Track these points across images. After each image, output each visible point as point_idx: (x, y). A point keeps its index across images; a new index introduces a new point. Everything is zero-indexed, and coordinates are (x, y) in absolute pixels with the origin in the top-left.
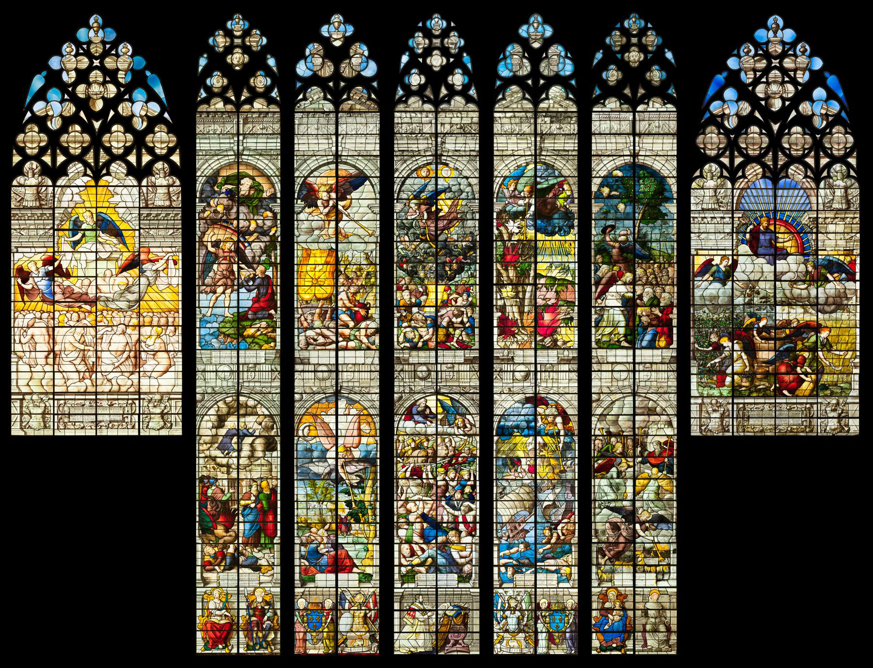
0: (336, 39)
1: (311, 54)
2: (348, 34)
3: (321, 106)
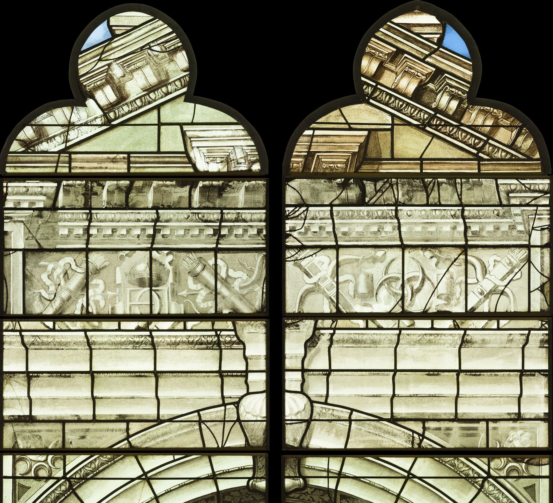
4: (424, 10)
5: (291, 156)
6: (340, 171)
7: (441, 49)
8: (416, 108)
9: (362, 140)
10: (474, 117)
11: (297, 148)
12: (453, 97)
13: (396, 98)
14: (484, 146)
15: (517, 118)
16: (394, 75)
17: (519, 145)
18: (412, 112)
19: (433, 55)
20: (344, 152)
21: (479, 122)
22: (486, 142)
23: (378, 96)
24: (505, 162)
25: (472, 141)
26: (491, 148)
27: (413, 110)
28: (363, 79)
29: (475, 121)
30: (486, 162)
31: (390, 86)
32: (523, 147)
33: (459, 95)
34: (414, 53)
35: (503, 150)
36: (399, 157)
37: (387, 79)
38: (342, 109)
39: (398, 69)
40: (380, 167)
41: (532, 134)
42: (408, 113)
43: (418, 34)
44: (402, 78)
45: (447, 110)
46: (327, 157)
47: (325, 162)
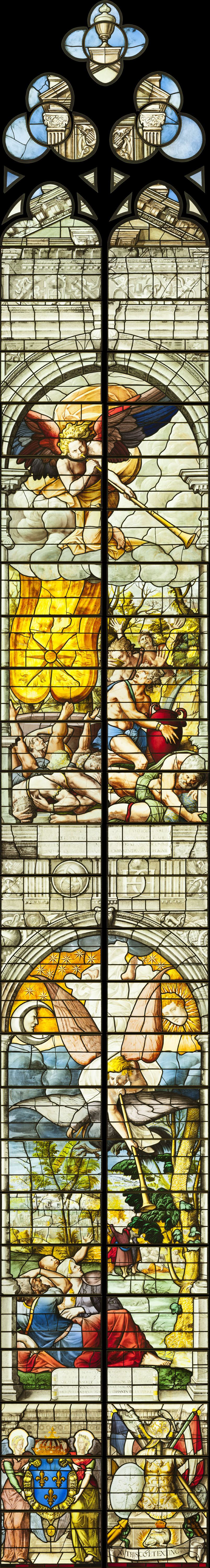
0: (102, 66)
1: (41, 103)
2: (132, 53)
3: (65, 233)
10: (180, 224)
12: (172, 217)
37: (147, 210)
41: (202, 230)
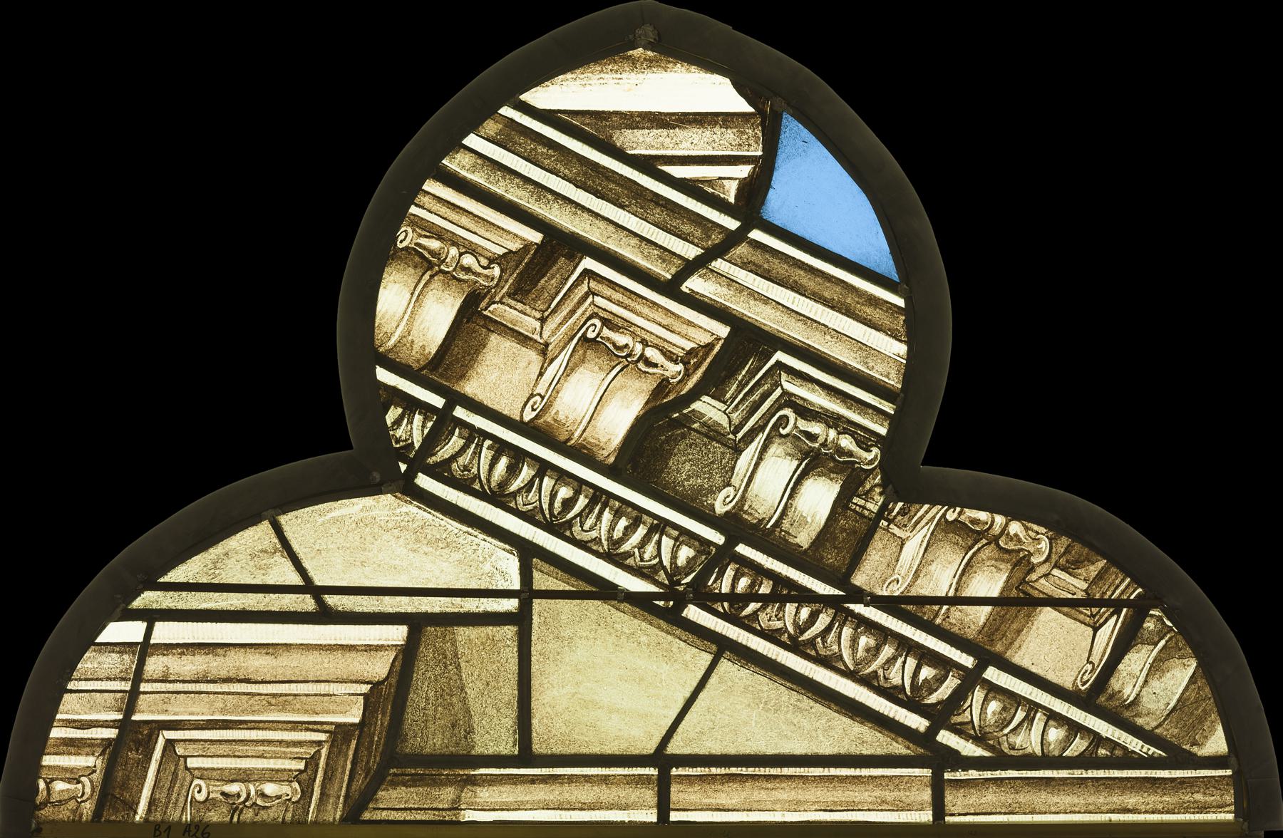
4: (676, 49)
5: (40, 744)
6: (274, 814)
7: (756, 235)
8: (639, 515)
9: (379, 667)
10: (915, 556)
11: (70, 707)
12: (814, 461)
13: (544, 468)
14: (959, 696)
15: (1120, 561)
16: (533, 357)
17: (1129, 692)
18: (618, 533)
19: (719, 265)
20: (295, 726)
21: (940, 581)
22: (971, 679)
23: (454, 458)
24: (1064, 774)
25: (902, 673)
26: (994, 706)
27: (623, 523)
28: (383, 375)
29: (917, 575)
30: (973, 774)
31: (512, 411)
32: (1148, 702)
33: (841, 451)
34: (628, 251)
35: (1052, 716)
36: (558, 749)
37: (501, 377)
38: (283, 519)
39: (553, 332)
40: (467, 795)
41: (1192, 637)
42: (597, 541)
43: (647, 165)
44: (569, 370)
45: (786, 524)
46: (213, 749)
47: (204, 774)
